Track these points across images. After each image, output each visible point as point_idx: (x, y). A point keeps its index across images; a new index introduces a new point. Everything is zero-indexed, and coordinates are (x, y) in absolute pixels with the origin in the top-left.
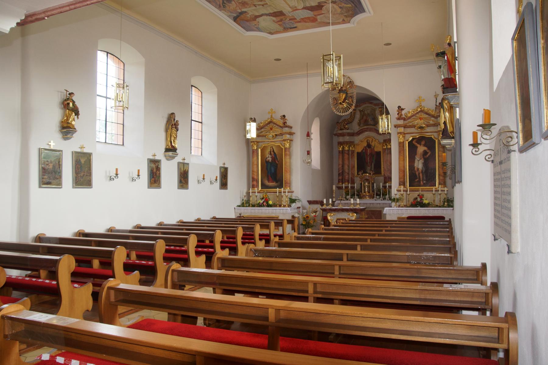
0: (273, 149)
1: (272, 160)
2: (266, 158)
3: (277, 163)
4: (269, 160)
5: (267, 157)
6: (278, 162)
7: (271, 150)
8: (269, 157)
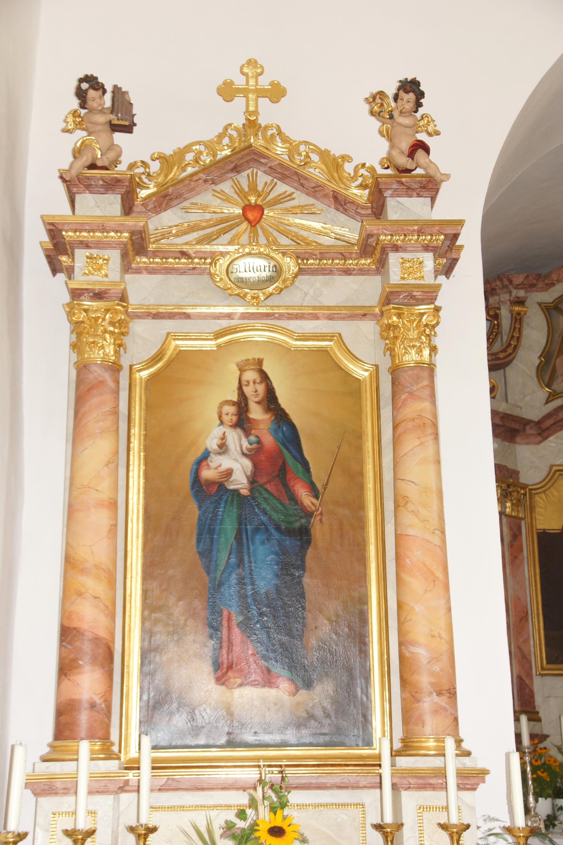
0: (265, 377)
1: (253, 480)
2: (199, 453)
3: (307, 499)
4: (229, 473)
5: (212, 444)
6: (315, 492)
7: (248, 391)
8: (223, 448)
